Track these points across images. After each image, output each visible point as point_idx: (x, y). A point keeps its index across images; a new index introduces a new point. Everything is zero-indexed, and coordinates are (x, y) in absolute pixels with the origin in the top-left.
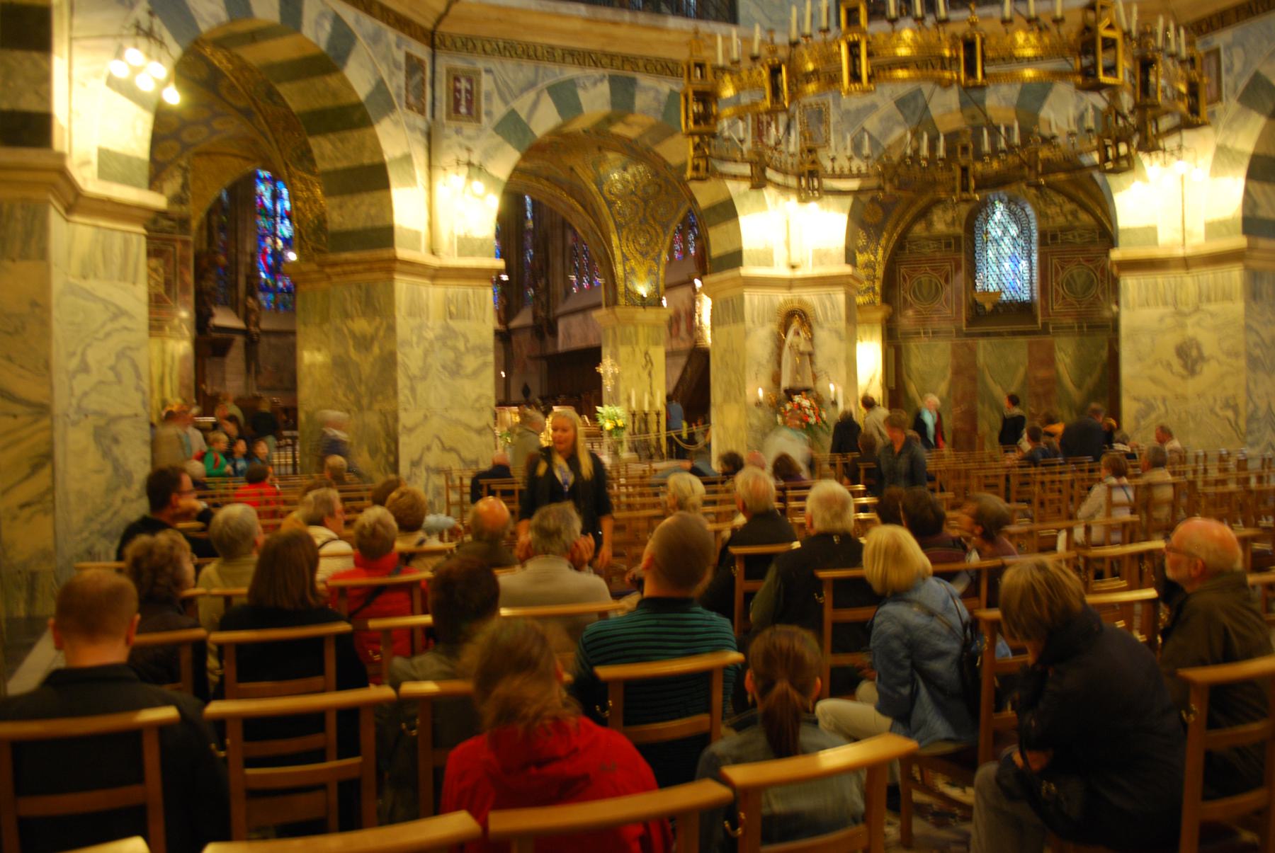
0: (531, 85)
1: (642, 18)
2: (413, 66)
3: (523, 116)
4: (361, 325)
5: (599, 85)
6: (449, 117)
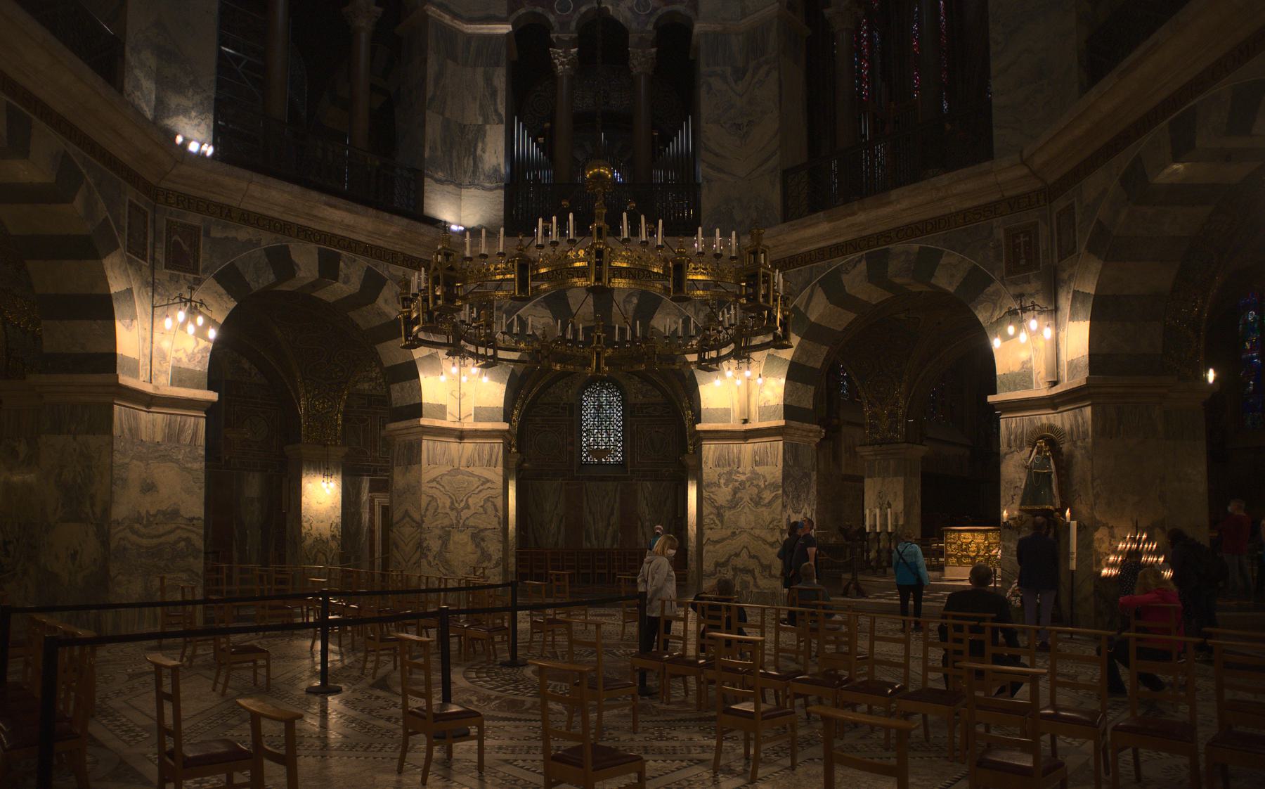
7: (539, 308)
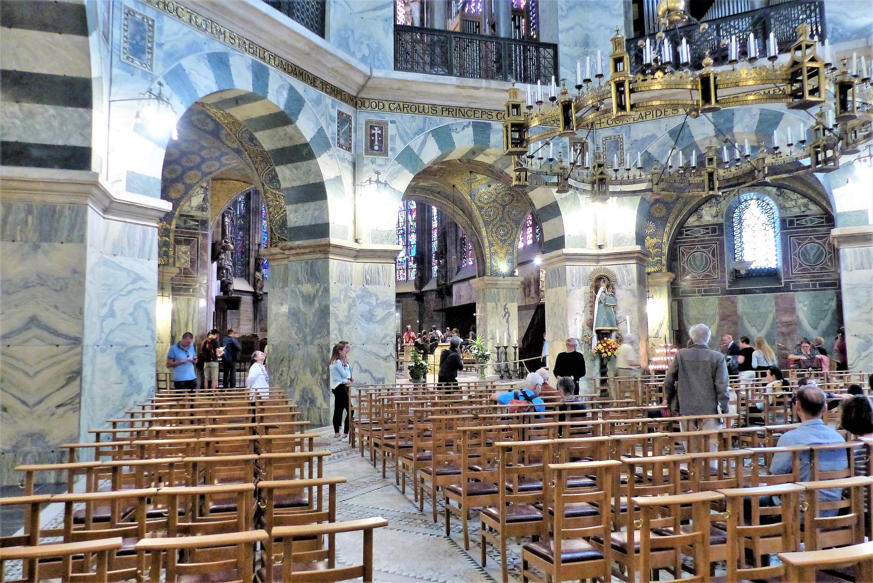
0: (422, 130)
2: (343, 120)
4: (307, 288)
5: (466, 129)
6: (367, 153)
7: (202, 65)
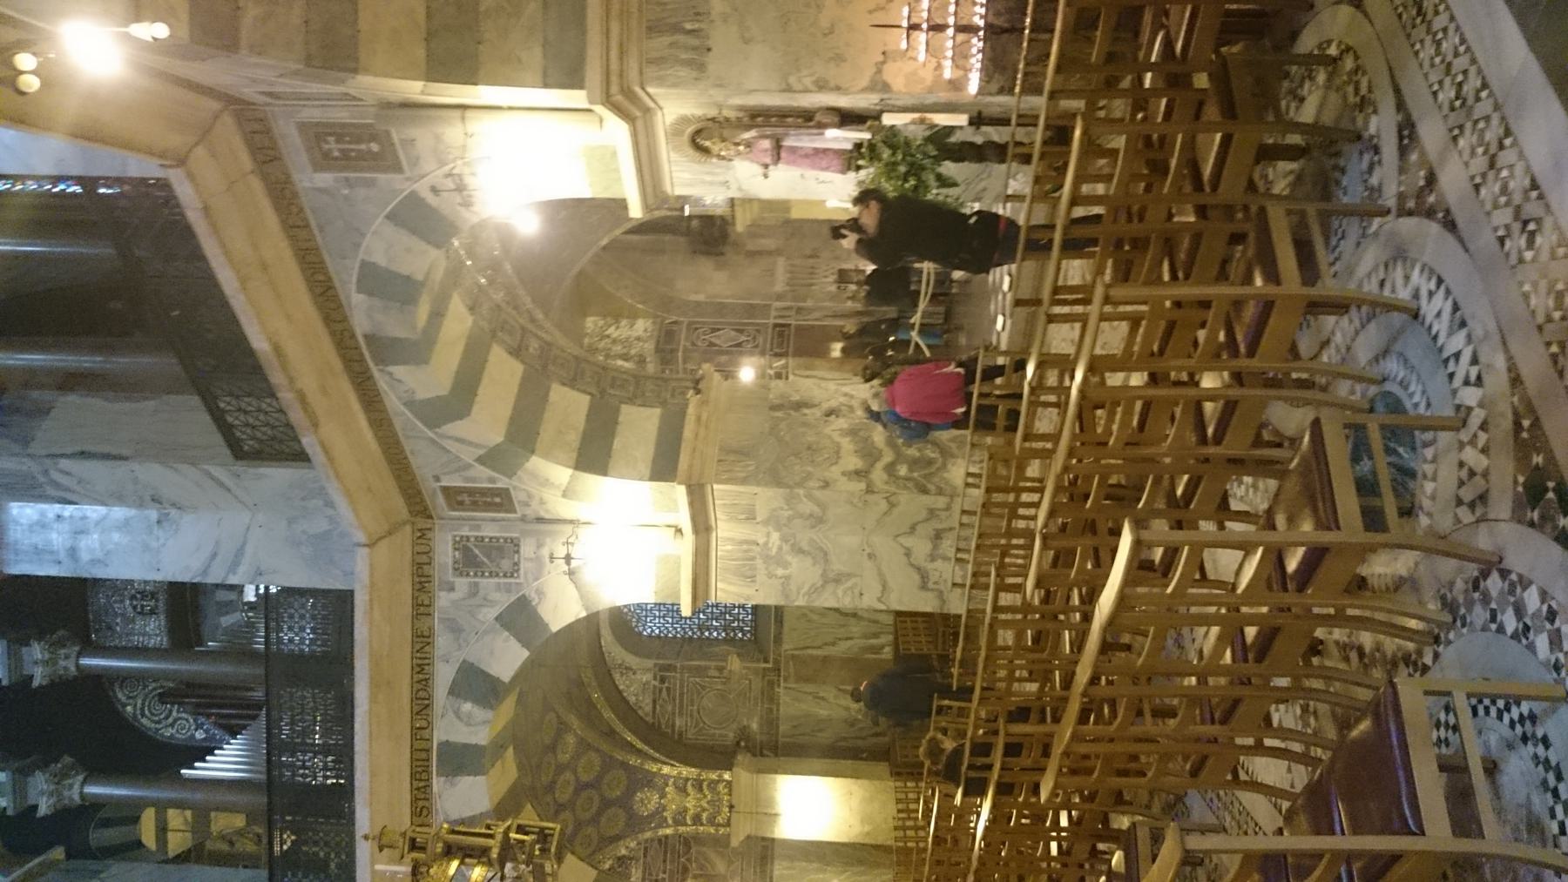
1: (276, 378)
3: (481, 452)
